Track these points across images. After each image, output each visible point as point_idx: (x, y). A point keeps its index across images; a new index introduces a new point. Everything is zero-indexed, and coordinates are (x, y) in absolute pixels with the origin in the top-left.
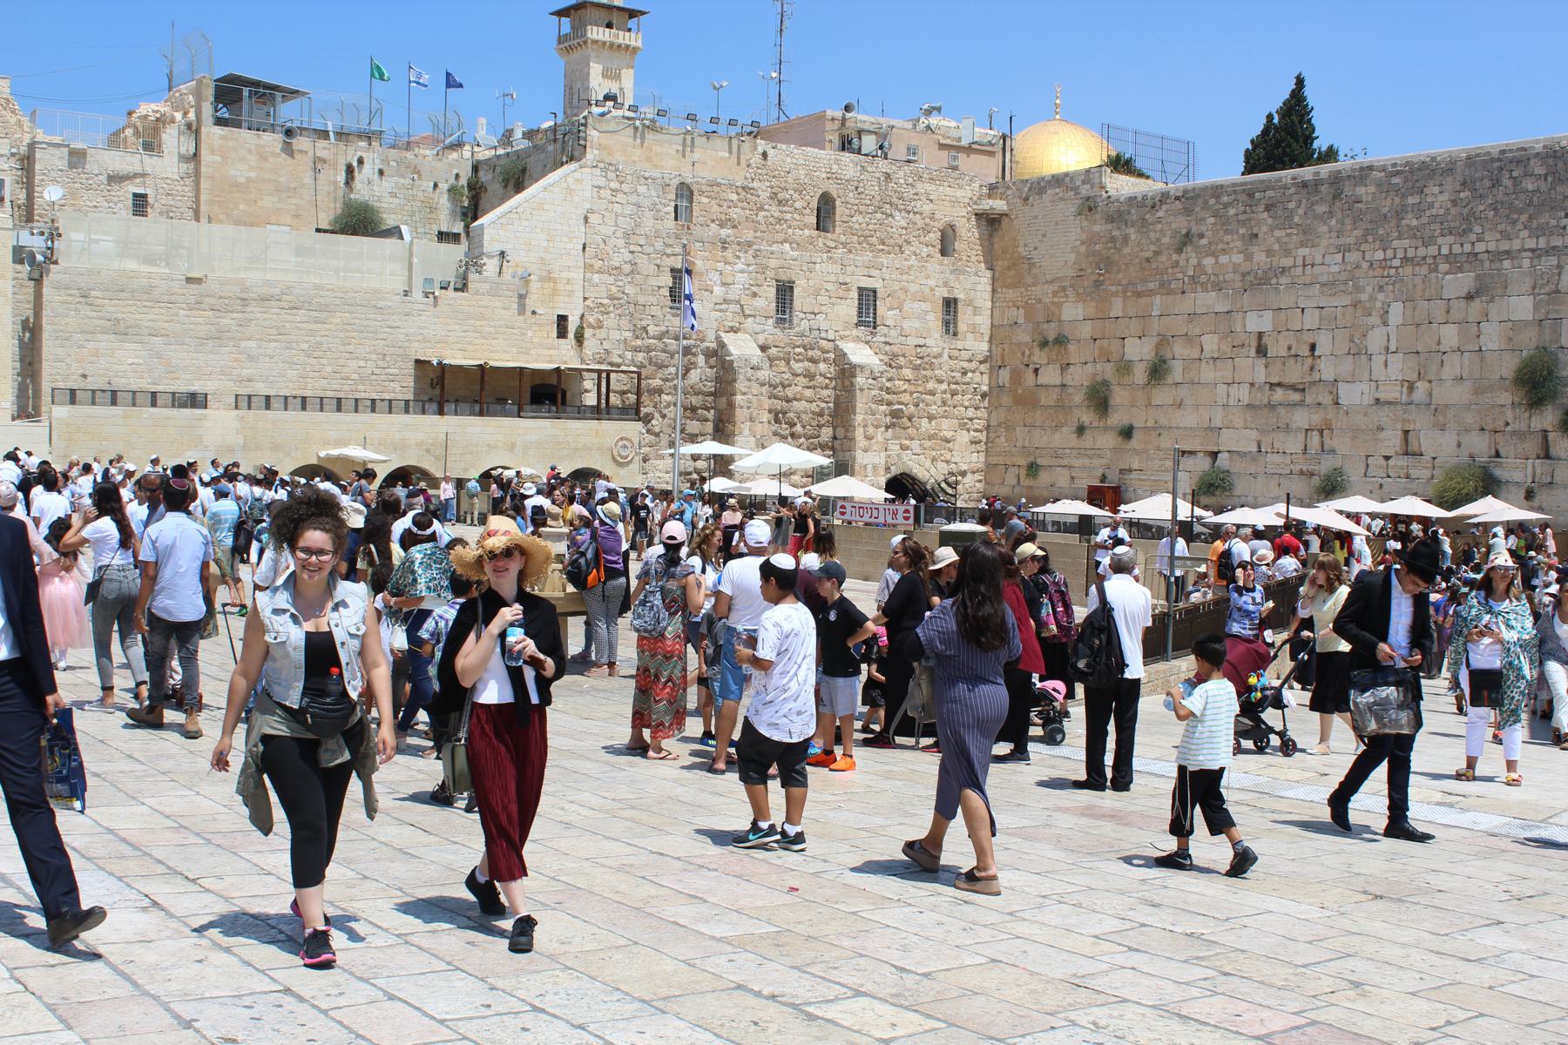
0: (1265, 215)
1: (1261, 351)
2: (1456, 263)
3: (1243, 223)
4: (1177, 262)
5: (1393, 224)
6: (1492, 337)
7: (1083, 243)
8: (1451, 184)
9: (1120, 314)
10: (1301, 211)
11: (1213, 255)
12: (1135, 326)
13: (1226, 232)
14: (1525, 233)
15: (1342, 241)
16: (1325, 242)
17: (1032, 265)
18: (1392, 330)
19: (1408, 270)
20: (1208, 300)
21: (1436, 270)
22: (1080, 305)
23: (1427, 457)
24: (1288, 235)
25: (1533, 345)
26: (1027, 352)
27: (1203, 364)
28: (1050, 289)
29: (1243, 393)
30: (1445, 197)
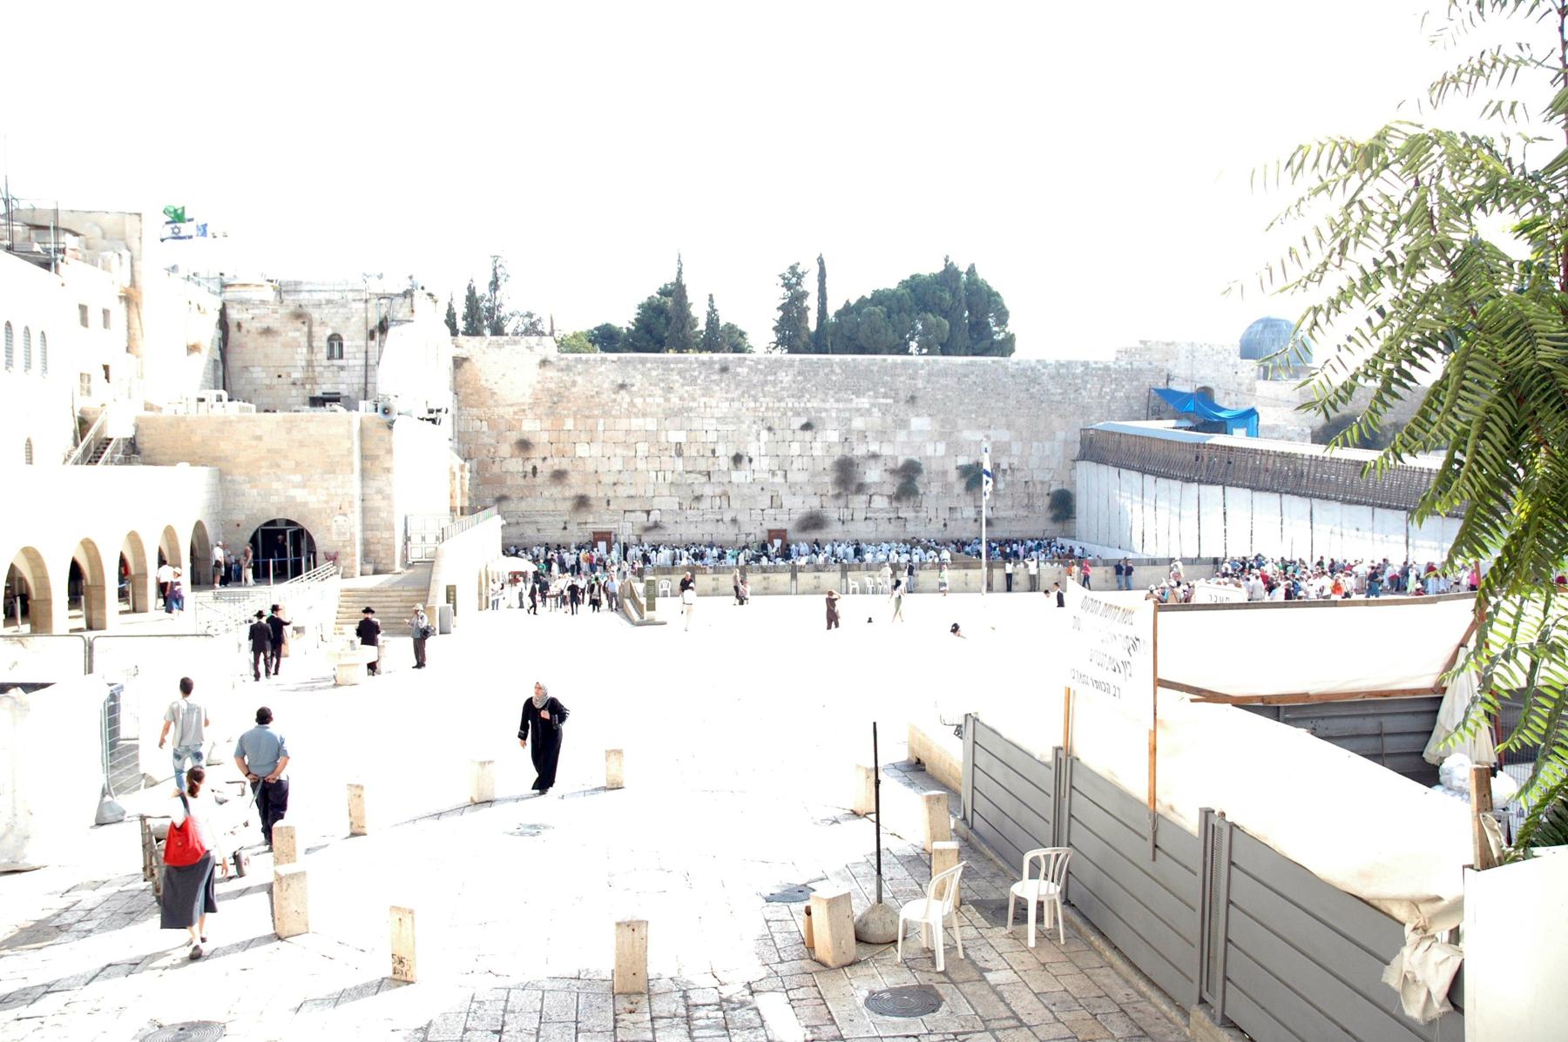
0: (678, 377)
2: (798, 414)
3: (662, 380)
4: (615, 401)
5: (760, 389)
6: (818, 450)
7: (539, 382)
8: (791, 372)
9: (572, 428)
10: (702, 377)
11: (642, 396)
12: (583, 436)
13: (651, 384)
14: (832, 400)
15: (730, 396)
16: (718, 395)
17: (493, 394)
18: (762, 443)
19: (770, 414)
20: (637, 423)
21: (784, 414)
22: (538, 421)
23: (786, 507)
24: (694, 390)
25: (840, 454)
26: (492, 450)
27: (638, 460)
28: (511, 410)
29: (669, 477)
30: (789, 378)
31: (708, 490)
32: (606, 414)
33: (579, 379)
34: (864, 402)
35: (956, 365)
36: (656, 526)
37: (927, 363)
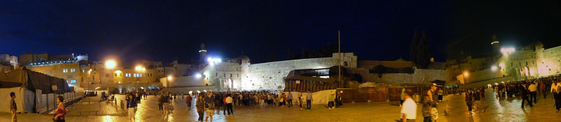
1: (264, 77)
2: (278, 71)
6: (281, 76)
31: (267, 83)
32: (255, 72)
33: (253, 68)
34: (287, 68)
35: (300, 61)
36: (261, 88)
37: (296, 61)
